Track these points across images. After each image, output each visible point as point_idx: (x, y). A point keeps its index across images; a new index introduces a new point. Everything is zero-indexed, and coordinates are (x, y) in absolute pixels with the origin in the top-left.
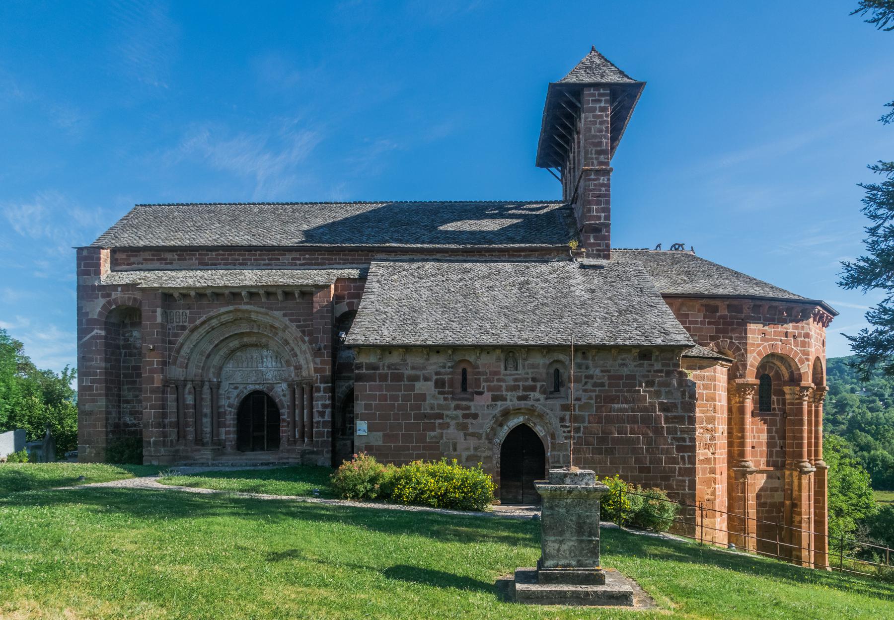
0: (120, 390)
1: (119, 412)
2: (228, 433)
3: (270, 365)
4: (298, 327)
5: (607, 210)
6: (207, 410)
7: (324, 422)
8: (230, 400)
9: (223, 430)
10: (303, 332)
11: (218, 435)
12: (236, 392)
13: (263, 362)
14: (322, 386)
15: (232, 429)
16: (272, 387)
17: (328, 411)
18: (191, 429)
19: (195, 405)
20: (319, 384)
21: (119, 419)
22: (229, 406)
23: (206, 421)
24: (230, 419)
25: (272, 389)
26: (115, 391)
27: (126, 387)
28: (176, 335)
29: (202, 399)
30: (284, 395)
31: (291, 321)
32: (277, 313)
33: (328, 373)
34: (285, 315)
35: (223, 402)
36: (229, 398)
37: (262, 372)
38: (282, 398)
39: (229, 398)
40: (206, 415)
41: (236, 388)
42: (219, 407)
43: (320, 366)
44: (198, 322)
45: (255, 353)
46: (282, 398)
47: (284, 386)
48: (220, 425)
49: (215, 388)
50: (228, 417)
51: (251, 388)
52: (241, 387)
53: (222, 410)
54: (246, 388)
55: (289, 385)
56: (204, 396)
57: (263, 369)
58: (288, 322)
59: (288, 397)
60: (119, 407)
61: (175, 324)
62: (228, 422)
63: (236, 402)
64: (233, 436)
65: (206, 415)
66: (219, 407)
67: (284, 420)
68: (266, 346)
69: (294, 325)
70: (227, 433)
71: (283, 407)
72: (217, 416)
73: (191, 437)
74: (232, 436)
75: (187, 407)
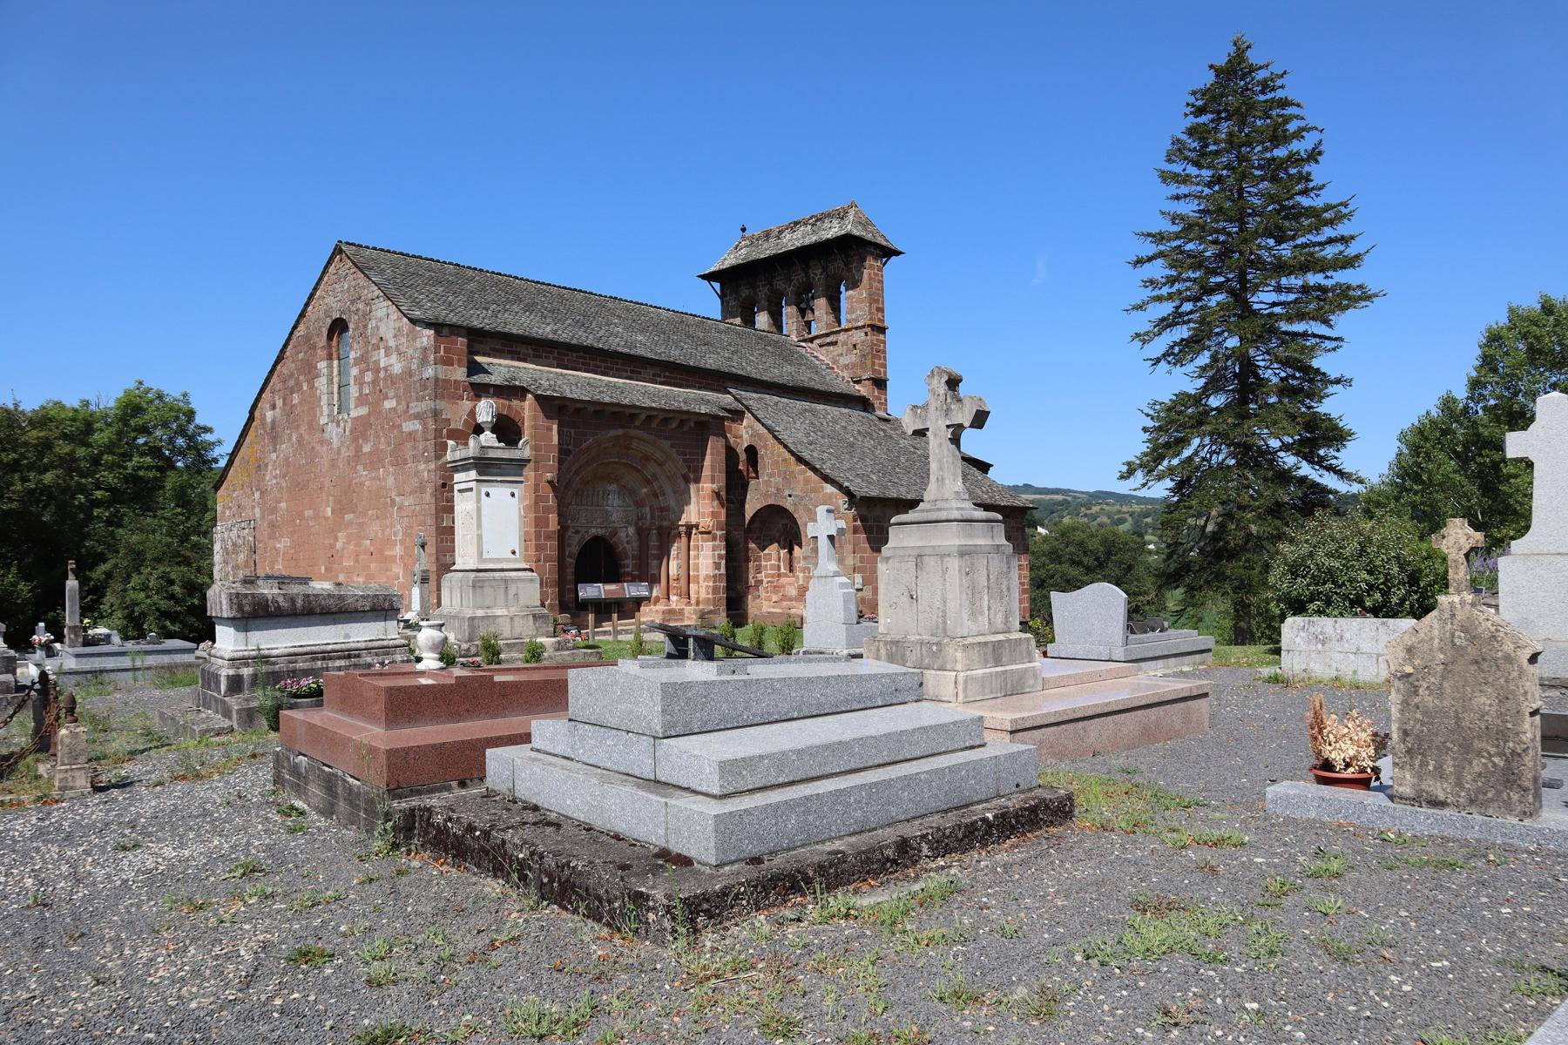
5: (884, 366)
25: (614, 533)
32: (666, 444)
33: (723, 518)
47: (631, 530)
52: (583, 531)
55: (639, 531)
68: (617, 480)
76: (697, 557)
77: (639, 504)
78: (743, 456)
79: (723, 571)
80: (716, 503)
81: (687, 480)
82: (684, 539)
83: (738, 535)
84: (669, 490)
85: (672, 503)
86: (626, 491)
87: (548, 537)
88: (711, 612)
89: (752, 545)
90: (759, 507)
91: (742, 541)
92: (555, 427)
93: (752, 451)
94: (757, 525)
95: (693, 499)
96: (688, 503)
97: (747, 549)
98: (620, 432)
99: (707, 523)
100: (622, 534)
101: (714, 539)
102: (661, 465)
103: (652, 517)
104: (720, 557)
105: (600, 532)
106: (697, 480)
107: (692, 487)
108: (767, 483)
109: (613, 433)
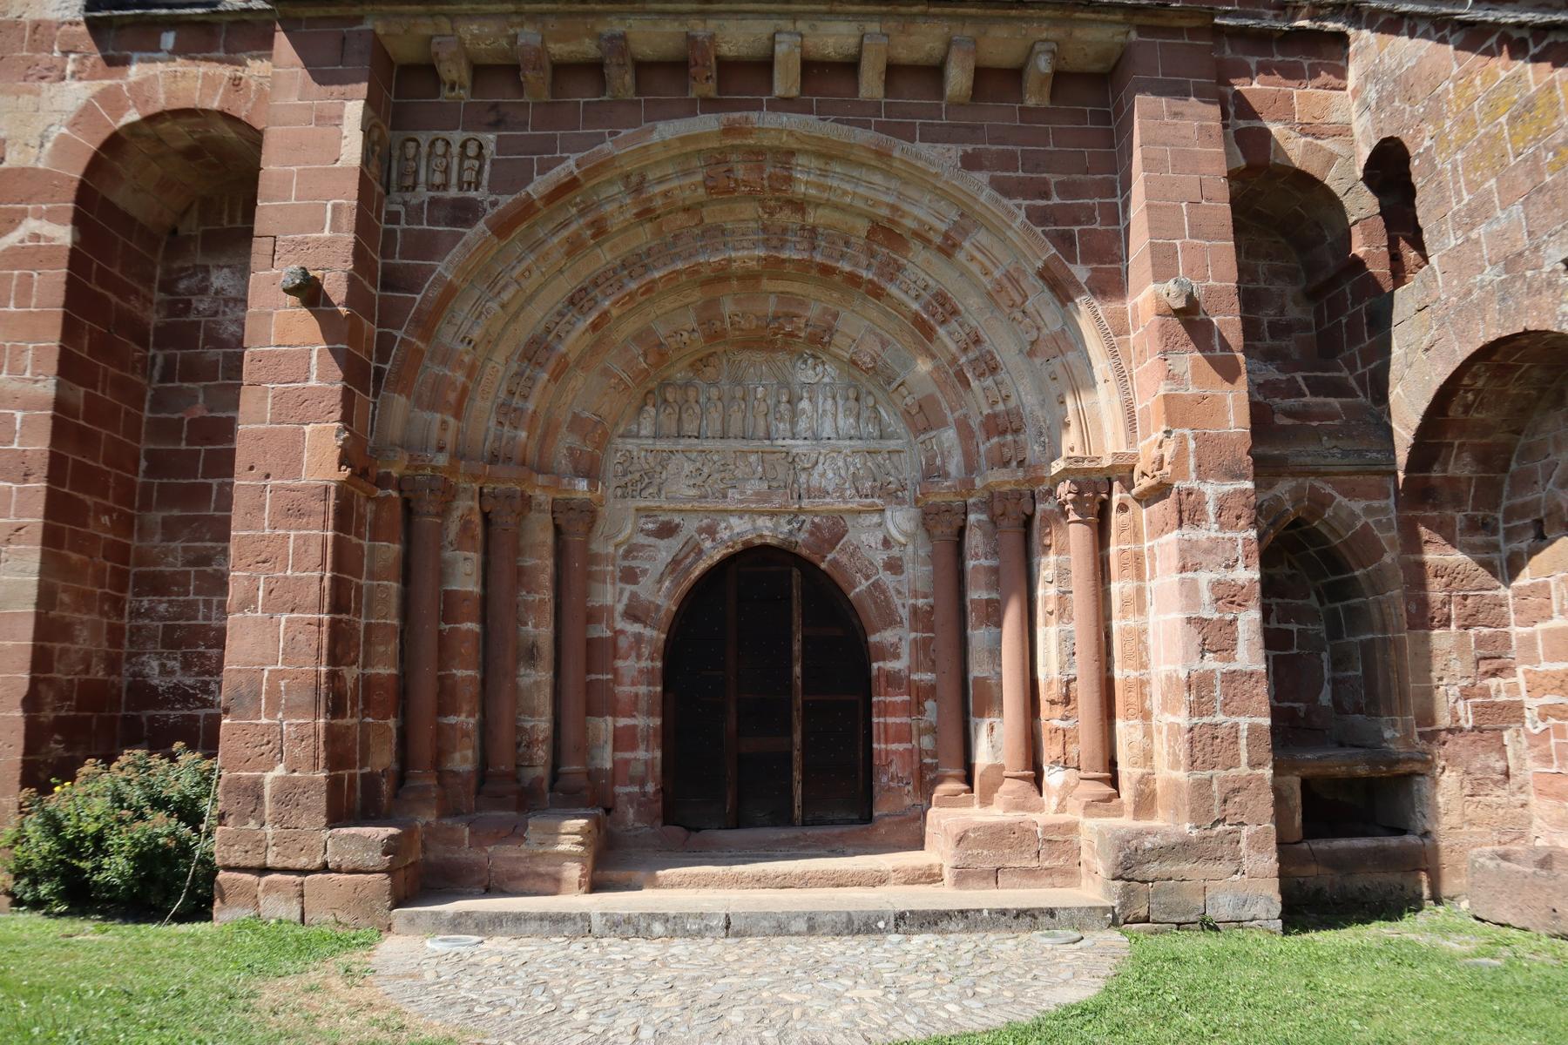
0: (126, 524)
1: (115, 634)
2: (627, 738)
3: (828, 430)
4: (1038, 217)
6: (539, 630)
7: (1231, 677)
8: (637, 591)
9: (605, 726)
10: (1064, 242)
11: (586, 748)
12: (665, 551)
13: (794, 415)
14: (1212, 490)
15: (640, 721)
16: (832, 532)
17: (1249, 620)
18: (465, 719)
19: (485, 600)
20: (1192, 483)
21: (113, 664)
22: (632, 614)
23: (536, 679)
24: (636, 673)
25: (832, 532)
26: (102, 527)
27: (157, 516)
28: (428, 247)
29: (520, 572)
30: (894, 566)
31: (1004, 189)
32: (941, 157)
34: (971, 162)
35: (610, 595)
36: (630, 576)
37: (792, 460)
38: (887, 578)
39: (630, 576)
40: (530, 655)
41: (667, 531)
42: (592, 616)
43: (1193, 390)
44: (538, 187)
45: (759, 372)
46: (887, 578)
47: (900, 521)
48: (599, 701)
49: (573, 527)
50: (628, 666)
51: (739, 529)
52: (690, 526)
53: (602, 631)
54: (711, 531)
55: (929, 517)
56: (529, 562)
57: (799, 446)
58: (986, 195)
59: (918, 572)
60: (117, 605)
61: (423, 194)
62: (625, 690)
63: (663, 596)
64: (647, 755)
65: (530, 655)
66: (592, 616)
67: (893, 680)
68: (819, 341)
69: (1018, 207)
70: (623, 739)
71: (890, 620)
72: (581, 658)
73: (463, 760)
74: (641, 754)
75: (449, 605)
76: (1139, 602)
77: (923, 418)
78: (1361, 205)
79: (1249, 655)
80: (1189, 360)
81: (1062, 290)
82: (1077, 535)
83: (1358, 511)
84: (1006, 349)
85: (1026, 396)
86: (868, 380)
87: (294, 512)
88: (1180, 850)
89: (1439, 555)
90: (1439, 374)
91: (1388, 537)
92: (354, 110)
93: (1390, 168)
94: (1459, 467)
95: (1101, 366)
96: (1081, 380)
97: (1417, 575)
98: (708, 123)
99: (1150, 449)
100: (865, 537)
101: (1188, 514)
102: (948, 248)
103: (970, 467)
104: (1228, 596)
105: (769, 530)
106: (1112, 285)
107: (1088, 315)
108: (1462, 262)
109: (667, 130)
